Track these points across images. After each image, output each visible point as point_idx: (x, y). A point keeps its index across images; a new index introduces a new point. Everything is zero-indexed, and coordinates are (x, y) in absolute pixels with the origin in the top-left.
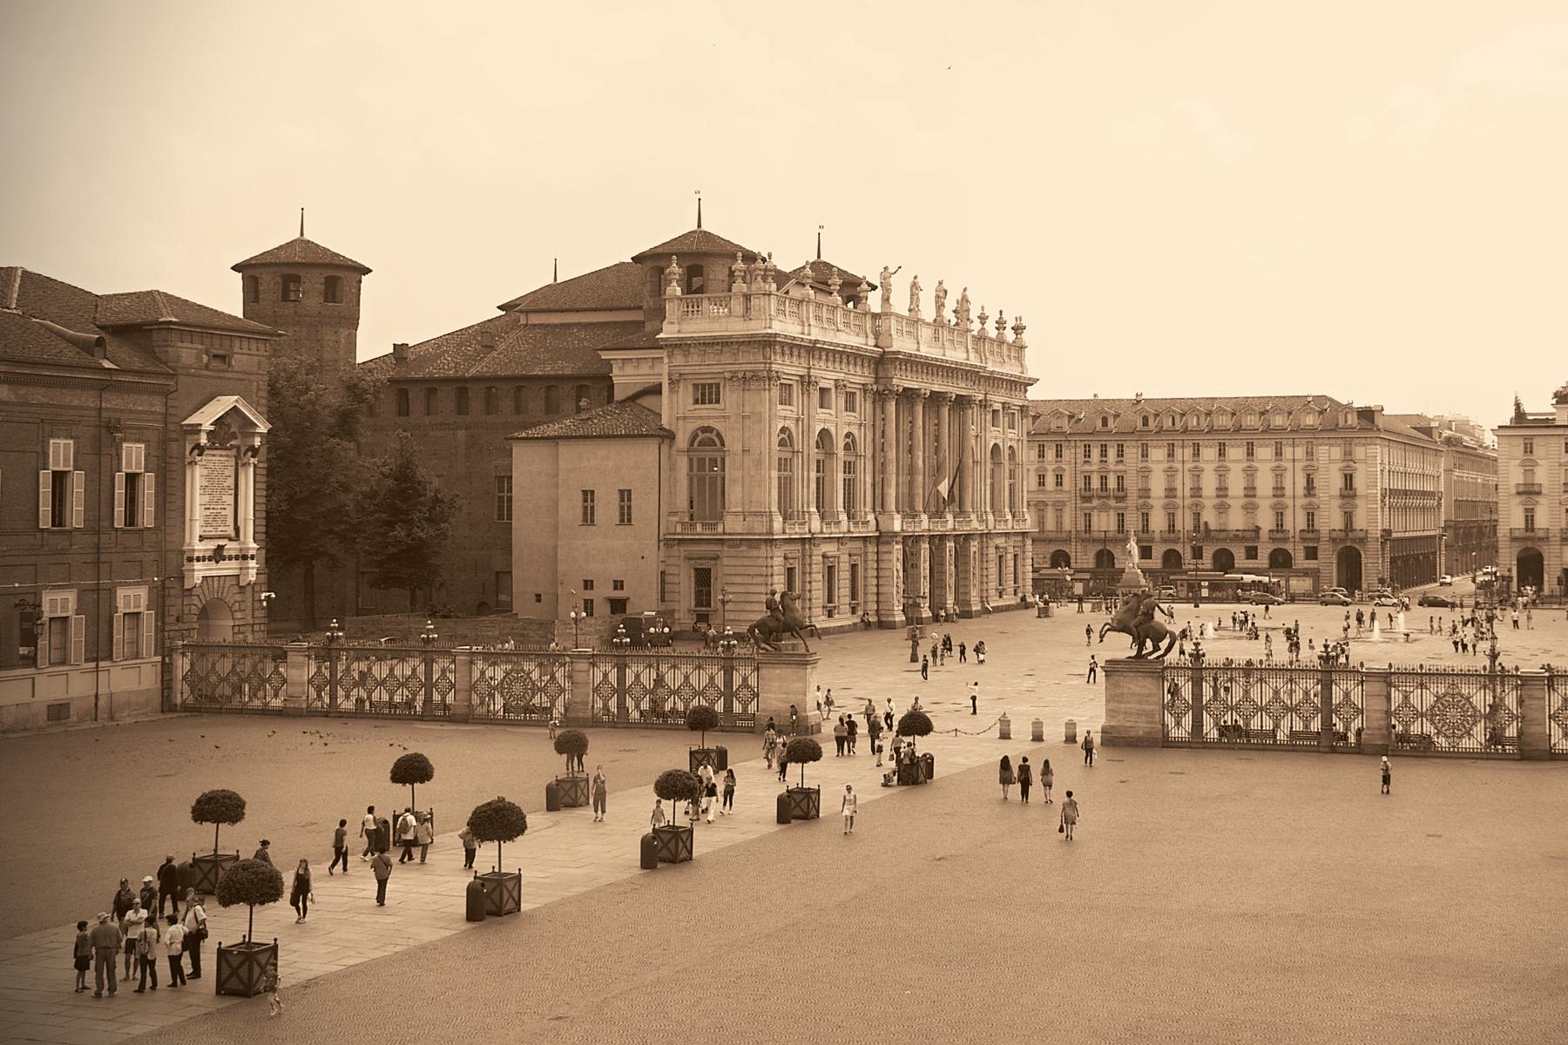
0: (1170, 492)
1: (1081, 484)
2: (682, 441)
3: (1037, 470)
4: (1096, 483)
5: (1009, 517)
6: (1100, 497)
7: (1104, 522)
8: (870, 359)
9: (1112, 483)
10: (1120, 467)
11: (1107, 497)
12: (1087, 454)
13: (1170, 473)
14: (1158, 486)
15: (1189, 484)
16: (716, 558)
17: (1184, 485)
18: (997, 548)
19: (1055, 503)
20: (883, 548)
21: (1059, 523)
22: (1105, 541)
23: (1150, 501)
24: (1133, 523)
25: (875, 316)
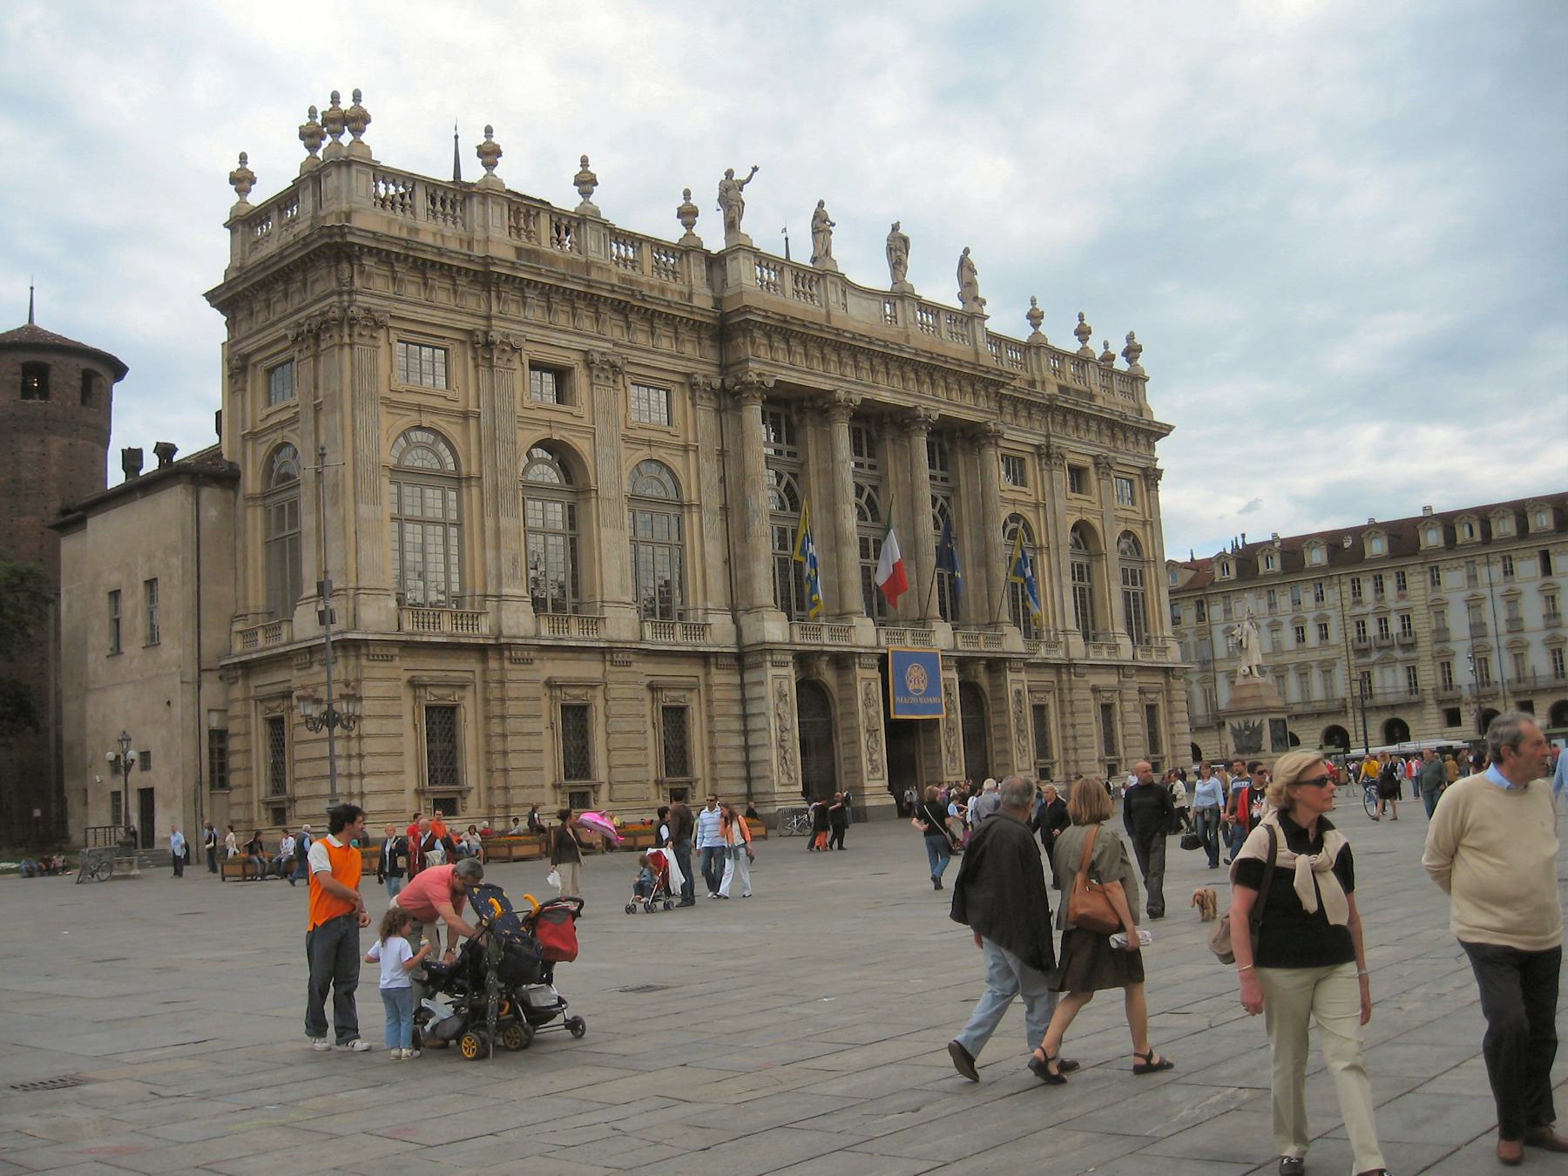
0: (1477, 629)
1: (1353, 634)
2: (252, 481)
3: (1293, 622)
4: (1372, 629)
5: (1125, 643)
6: (1380, 648)
7: (1389, 682)
8: (696, 327)
9: (1395, 626)
10: (1404, 604)
11: (1391, 647)
12: (1357, 592)
13: (1474, 604)
14: (1458, 622)
15: (1503, 615)
16: (287, 695)
17: (1495, 617)
18: (1095, 690)
19: (1321, 663)
20: (750, 677)
21: (1328, 687)
22: (1393, 707)
23: (1452, 646)
24: (1429, 676)
25: (715, 262)
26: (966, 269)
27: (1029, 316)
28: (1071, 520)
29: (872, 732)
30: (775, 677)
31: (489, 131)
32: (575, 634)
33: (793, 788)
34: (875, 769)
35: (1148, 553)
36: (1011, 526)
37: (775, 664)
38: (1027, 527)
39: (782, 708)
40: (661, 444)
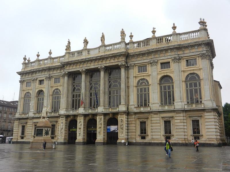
8: (61, 68)
18: (162, 118)
26: (123, 33)
27: (152, 32)
28: (160, 77)
29: (80, 128)
30: (61, 120)
31: (38, 53)
32: (37, 115)
33: (62, 138)
34: (80, 135)
35: (201, 78)
36: (141, 81)
37: (62, 118)
38: (147, 81)
39: (61, 124)
40: (58, 86)
